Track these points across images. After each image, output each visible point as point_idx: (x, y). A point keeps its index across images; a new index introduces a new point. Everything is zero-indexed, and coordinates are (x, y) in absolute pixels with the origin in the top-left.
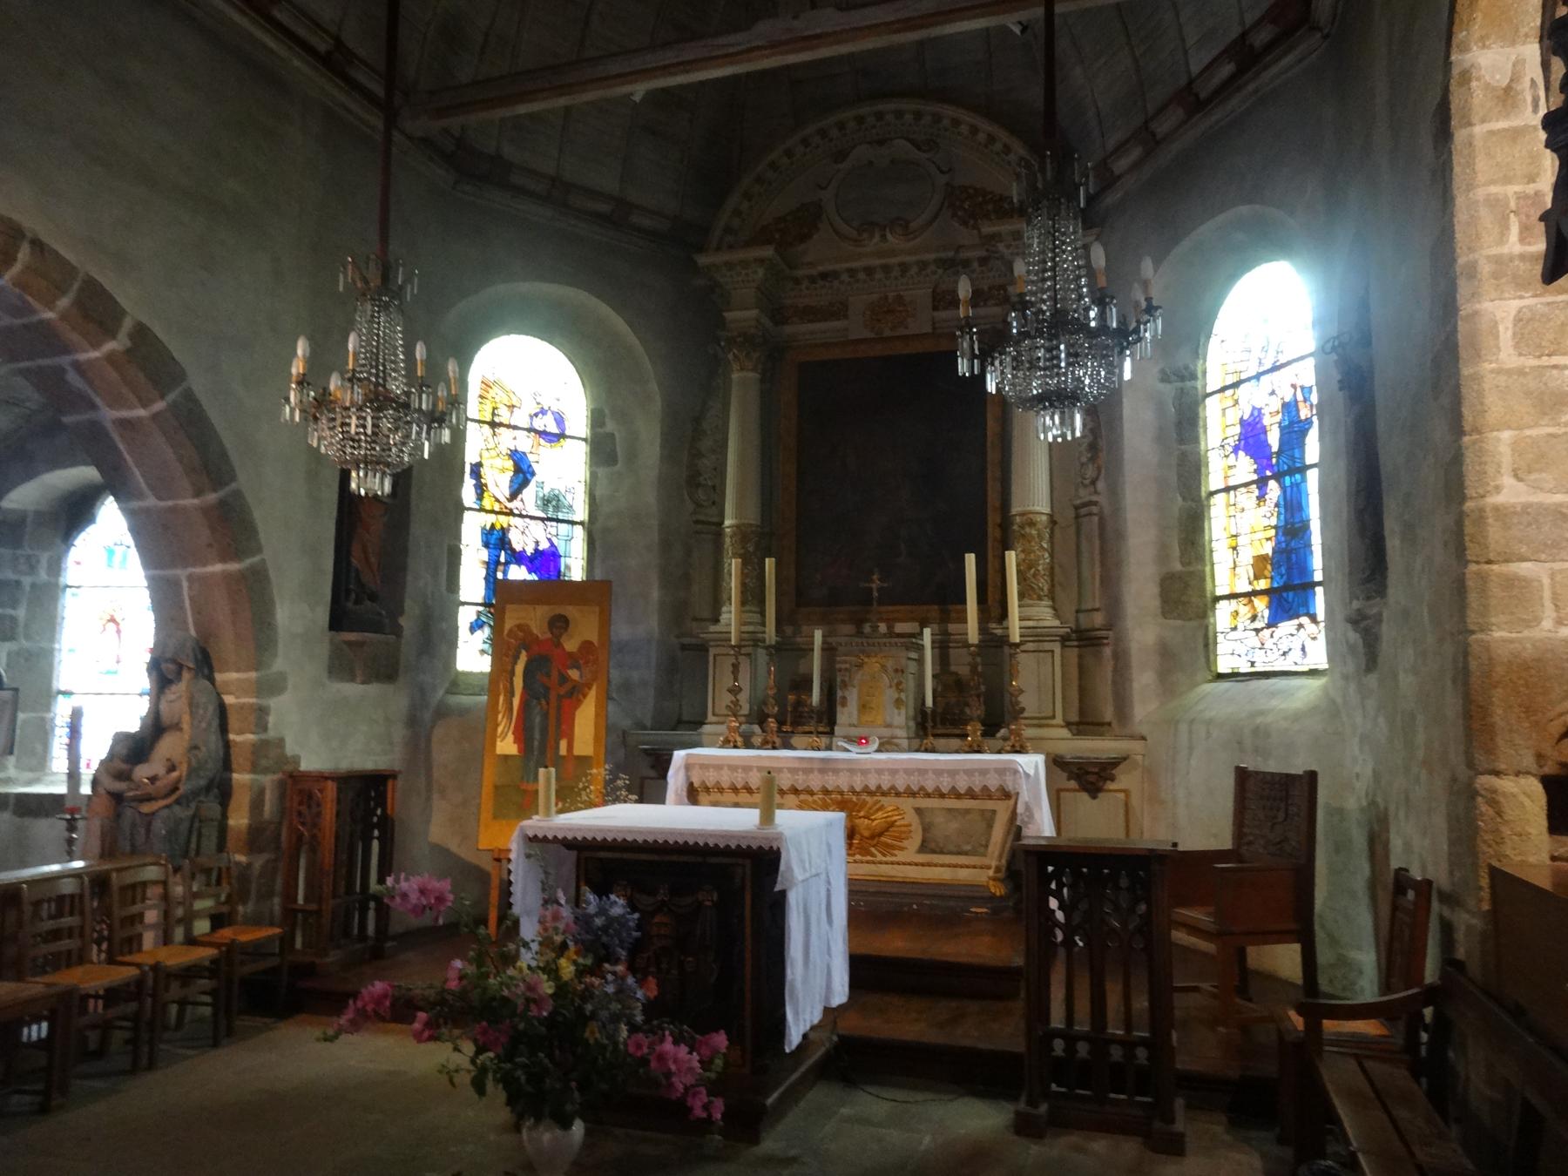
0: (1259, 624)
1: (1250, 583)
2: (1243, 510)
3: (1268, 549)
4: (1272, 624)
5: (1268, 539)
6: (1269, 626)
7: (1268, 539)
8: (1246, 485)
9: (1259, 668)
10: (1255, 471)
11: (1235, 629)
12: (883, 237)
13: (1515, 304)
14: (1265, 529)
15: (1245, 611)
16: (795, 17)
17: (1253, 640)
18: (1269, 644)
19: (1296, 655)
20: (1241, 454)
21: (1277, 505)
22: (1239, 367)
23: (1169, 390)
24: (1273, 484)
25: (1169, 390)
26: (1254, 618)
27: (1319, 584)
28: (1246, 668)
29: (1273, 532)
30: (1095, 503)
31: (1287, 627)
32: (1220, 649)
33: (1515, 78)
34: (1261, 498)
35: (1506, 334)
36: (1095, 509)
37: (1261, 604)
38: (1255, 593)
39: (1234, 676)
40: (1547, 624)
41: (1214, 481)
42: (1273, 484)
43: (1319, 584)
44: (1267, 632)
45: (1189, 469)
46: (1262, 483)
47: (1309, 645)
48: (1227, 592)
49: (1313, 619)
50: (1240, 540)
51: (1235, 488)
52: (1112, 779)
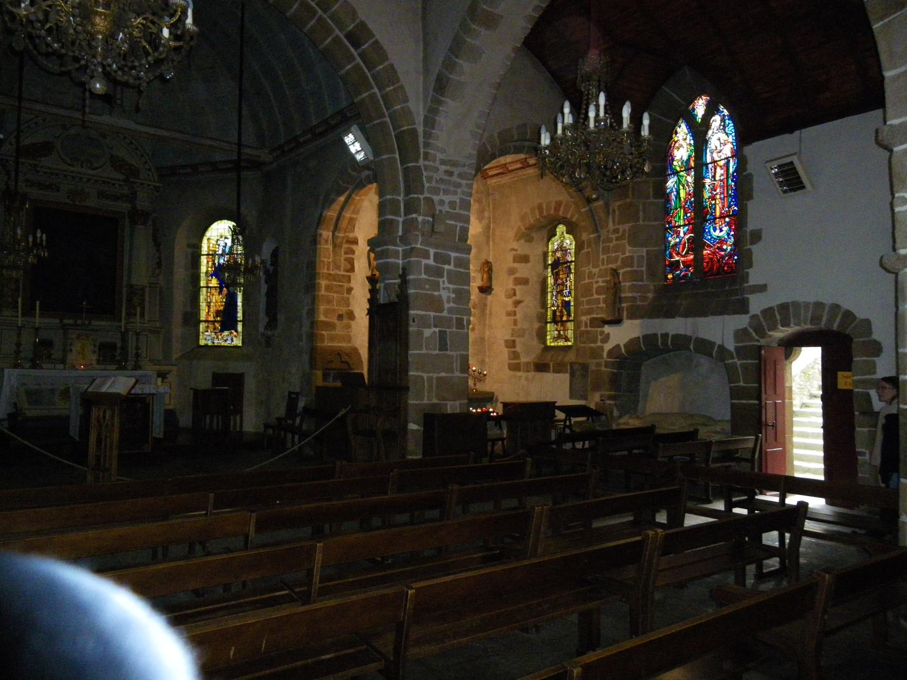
0: (216, 331)
1: (214, 318)
2: (213, 295)
3: (222, 308)
4: (222, 331)
5: (222, 305)
6: (220, 332)
7: (222, 305)
8: (215, 287)
9: (216, 344)
10: (219, 284)
11: (207, 331)
12: (82, 166)
13: (325, 282)
14: (221, 302)
15: (210, 326)
16: (119, 119)
17: (213, 335)
18: (220, 337)
19: (229, 342)
20: (214, 277)
21: (226, 295)
22: (217, 250)
23: (190, 250)
24: (225, 289)
25: (190, 250)
26: (215, 329)
27: (240, 321)
28: (210, 343)
29: (224, 304)
30: (158, 284)
31: (226, 333)
32: (201, 337)
33: (328, 238)
34: (220, 293)
35: (323, 288)
36: (158, 286)
37: (217, 325)
38: (216, 321)
39: (206, 346)
40: (326, 342)
41: (203, 283)
42: (225, 289)
43: (240, 321)
44: (219, 334)
45: (196, 278)
46: (221, 289)
47: (234, 339)
48: (204, 319)
49: (236, 331)
50: (212, 304)
51: (211, 287)
52: (166, 378)
